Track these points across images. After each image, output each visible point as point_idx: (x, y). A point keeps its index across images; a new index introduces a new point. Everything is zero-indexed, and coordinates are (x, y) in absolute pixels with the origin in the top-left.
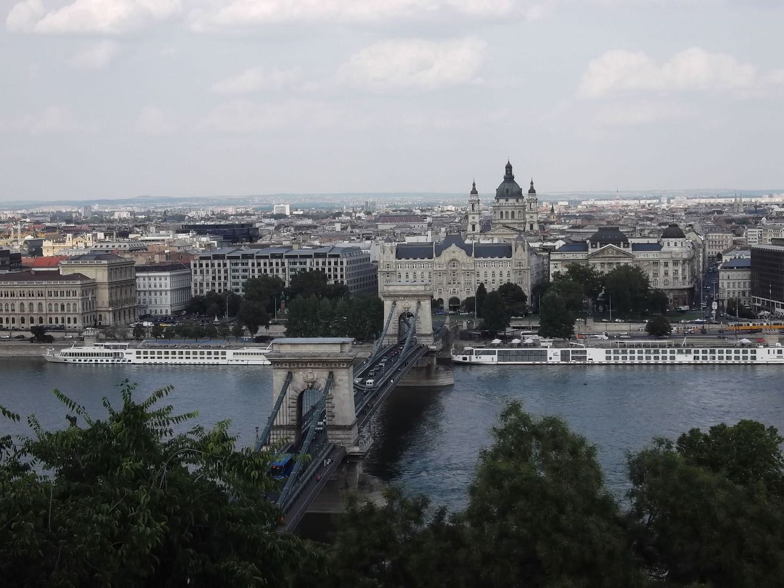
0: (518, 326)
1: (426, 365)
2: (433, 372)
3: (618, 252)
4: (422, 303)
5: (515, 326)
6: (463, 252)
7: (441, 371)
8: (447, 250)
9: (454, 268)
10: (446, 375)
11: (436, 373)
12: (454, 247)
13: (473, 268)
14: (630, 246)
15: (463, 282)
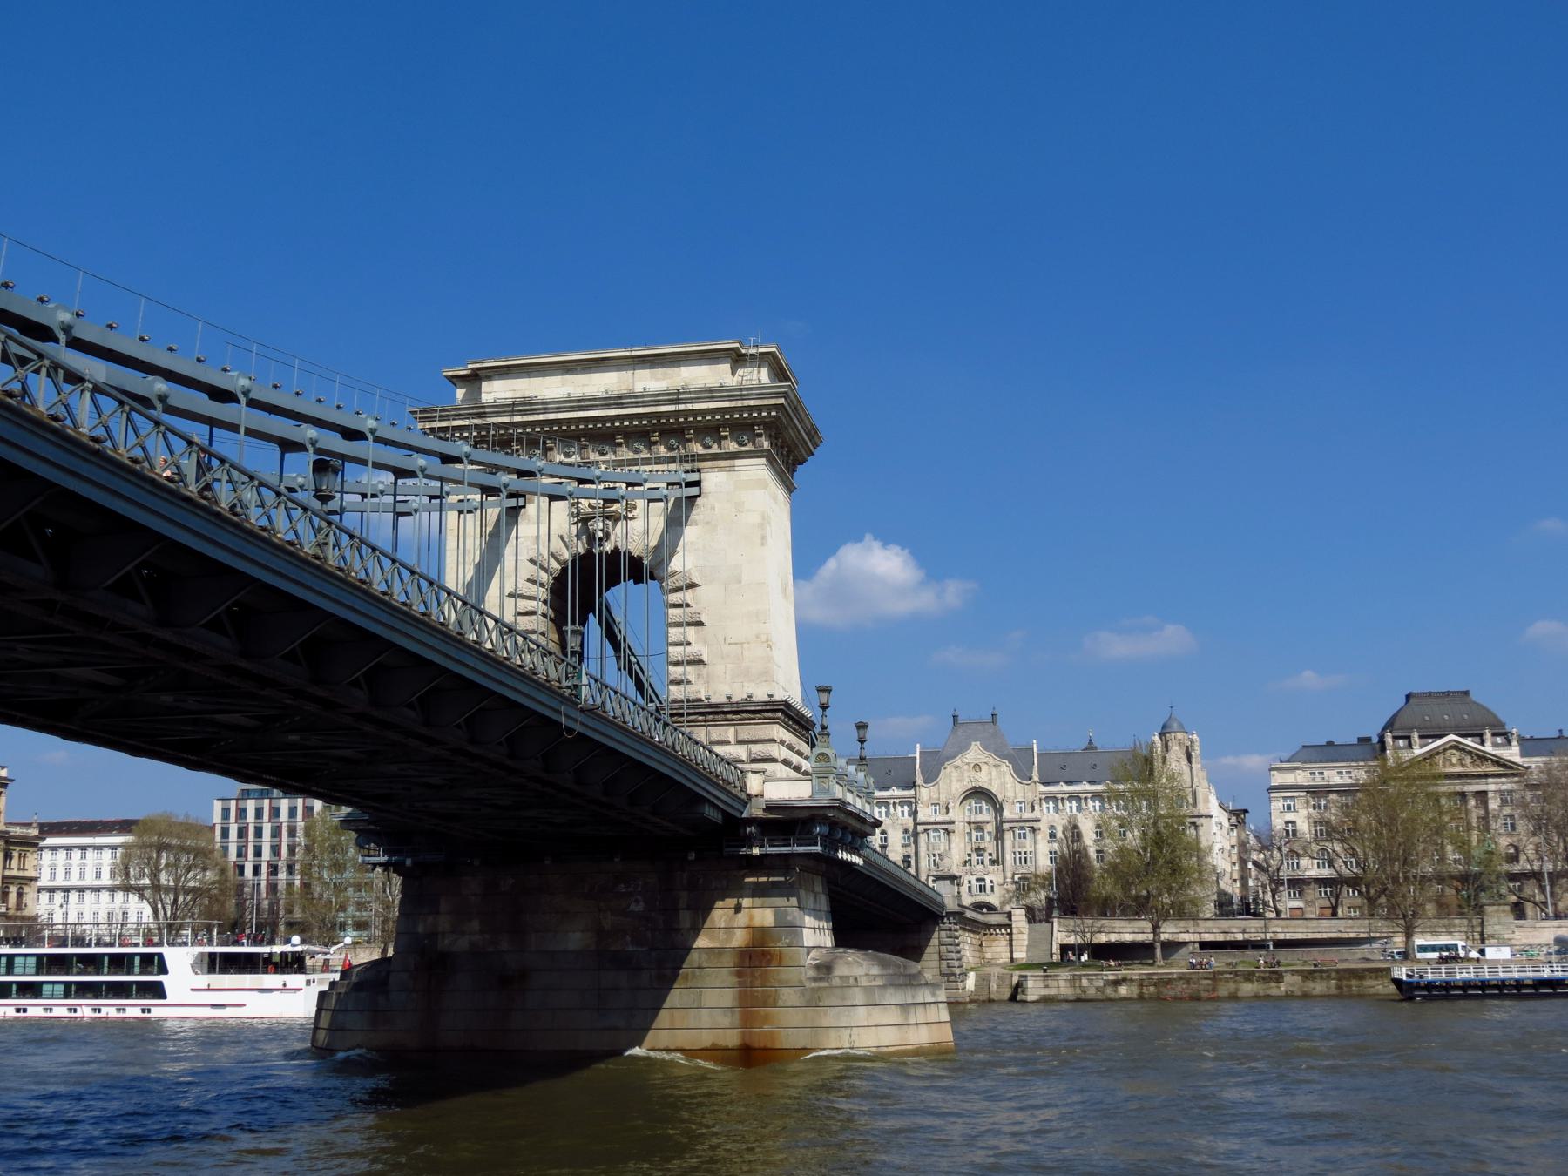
0: (1221, 938)
1: (739, 939)
2: (788, 996)
3: (1482, 758)
4: (713, 479)
5: (1207, 937)
6: (1006, 767)
7: (848, 983)
8: (957, 762)
9: (980, 818)
10: (894, 1016)
11: (813, 1001)
12: (975, 752)
13: (1037, 814)
14: (1514, 743)
15: (1009, 857)
